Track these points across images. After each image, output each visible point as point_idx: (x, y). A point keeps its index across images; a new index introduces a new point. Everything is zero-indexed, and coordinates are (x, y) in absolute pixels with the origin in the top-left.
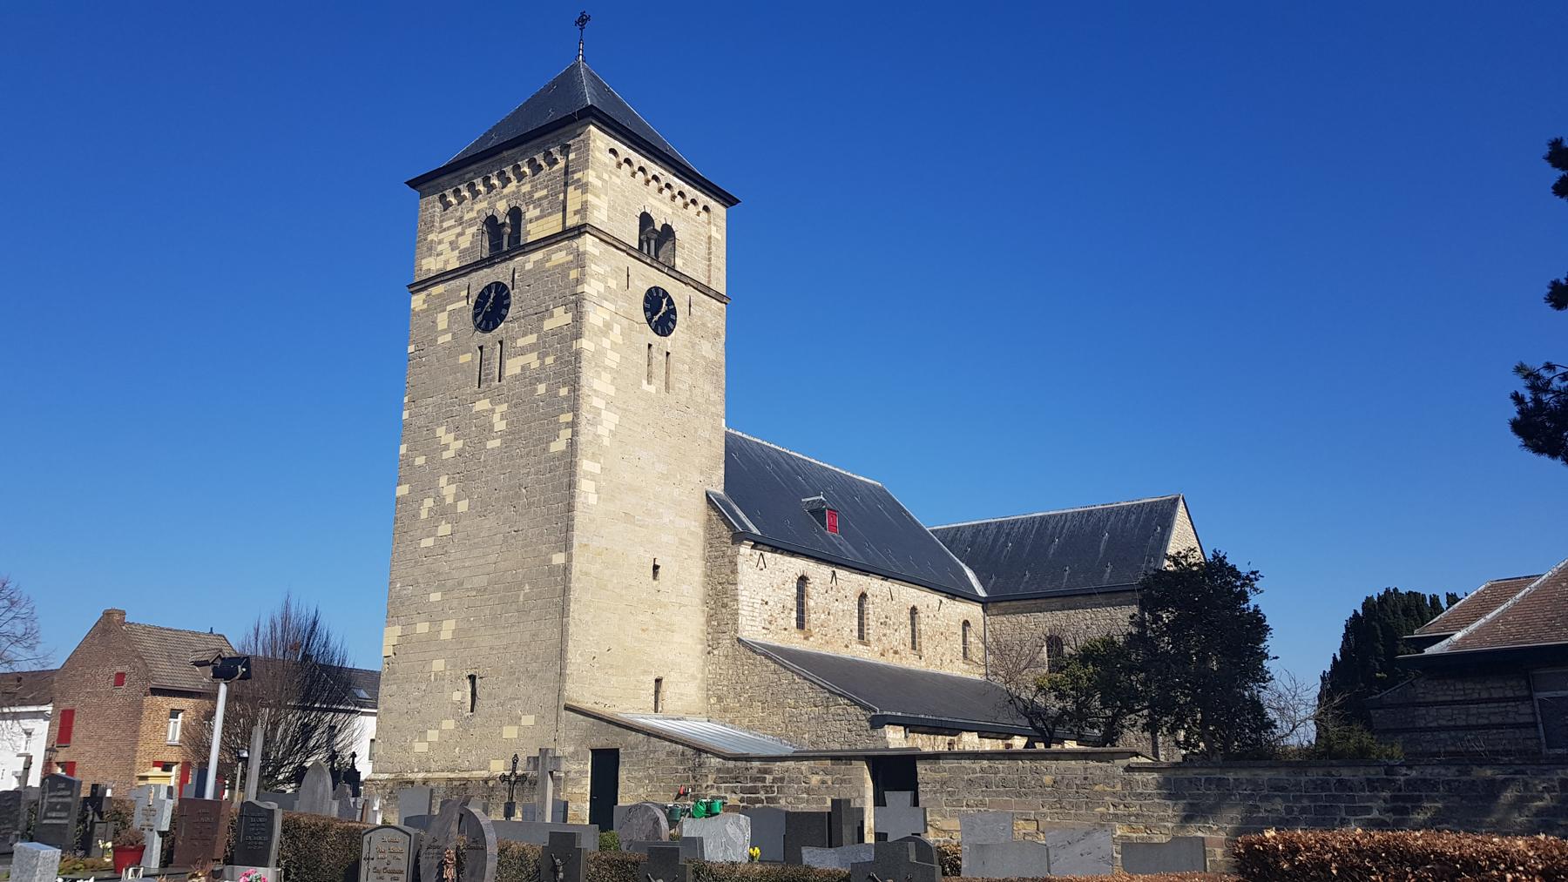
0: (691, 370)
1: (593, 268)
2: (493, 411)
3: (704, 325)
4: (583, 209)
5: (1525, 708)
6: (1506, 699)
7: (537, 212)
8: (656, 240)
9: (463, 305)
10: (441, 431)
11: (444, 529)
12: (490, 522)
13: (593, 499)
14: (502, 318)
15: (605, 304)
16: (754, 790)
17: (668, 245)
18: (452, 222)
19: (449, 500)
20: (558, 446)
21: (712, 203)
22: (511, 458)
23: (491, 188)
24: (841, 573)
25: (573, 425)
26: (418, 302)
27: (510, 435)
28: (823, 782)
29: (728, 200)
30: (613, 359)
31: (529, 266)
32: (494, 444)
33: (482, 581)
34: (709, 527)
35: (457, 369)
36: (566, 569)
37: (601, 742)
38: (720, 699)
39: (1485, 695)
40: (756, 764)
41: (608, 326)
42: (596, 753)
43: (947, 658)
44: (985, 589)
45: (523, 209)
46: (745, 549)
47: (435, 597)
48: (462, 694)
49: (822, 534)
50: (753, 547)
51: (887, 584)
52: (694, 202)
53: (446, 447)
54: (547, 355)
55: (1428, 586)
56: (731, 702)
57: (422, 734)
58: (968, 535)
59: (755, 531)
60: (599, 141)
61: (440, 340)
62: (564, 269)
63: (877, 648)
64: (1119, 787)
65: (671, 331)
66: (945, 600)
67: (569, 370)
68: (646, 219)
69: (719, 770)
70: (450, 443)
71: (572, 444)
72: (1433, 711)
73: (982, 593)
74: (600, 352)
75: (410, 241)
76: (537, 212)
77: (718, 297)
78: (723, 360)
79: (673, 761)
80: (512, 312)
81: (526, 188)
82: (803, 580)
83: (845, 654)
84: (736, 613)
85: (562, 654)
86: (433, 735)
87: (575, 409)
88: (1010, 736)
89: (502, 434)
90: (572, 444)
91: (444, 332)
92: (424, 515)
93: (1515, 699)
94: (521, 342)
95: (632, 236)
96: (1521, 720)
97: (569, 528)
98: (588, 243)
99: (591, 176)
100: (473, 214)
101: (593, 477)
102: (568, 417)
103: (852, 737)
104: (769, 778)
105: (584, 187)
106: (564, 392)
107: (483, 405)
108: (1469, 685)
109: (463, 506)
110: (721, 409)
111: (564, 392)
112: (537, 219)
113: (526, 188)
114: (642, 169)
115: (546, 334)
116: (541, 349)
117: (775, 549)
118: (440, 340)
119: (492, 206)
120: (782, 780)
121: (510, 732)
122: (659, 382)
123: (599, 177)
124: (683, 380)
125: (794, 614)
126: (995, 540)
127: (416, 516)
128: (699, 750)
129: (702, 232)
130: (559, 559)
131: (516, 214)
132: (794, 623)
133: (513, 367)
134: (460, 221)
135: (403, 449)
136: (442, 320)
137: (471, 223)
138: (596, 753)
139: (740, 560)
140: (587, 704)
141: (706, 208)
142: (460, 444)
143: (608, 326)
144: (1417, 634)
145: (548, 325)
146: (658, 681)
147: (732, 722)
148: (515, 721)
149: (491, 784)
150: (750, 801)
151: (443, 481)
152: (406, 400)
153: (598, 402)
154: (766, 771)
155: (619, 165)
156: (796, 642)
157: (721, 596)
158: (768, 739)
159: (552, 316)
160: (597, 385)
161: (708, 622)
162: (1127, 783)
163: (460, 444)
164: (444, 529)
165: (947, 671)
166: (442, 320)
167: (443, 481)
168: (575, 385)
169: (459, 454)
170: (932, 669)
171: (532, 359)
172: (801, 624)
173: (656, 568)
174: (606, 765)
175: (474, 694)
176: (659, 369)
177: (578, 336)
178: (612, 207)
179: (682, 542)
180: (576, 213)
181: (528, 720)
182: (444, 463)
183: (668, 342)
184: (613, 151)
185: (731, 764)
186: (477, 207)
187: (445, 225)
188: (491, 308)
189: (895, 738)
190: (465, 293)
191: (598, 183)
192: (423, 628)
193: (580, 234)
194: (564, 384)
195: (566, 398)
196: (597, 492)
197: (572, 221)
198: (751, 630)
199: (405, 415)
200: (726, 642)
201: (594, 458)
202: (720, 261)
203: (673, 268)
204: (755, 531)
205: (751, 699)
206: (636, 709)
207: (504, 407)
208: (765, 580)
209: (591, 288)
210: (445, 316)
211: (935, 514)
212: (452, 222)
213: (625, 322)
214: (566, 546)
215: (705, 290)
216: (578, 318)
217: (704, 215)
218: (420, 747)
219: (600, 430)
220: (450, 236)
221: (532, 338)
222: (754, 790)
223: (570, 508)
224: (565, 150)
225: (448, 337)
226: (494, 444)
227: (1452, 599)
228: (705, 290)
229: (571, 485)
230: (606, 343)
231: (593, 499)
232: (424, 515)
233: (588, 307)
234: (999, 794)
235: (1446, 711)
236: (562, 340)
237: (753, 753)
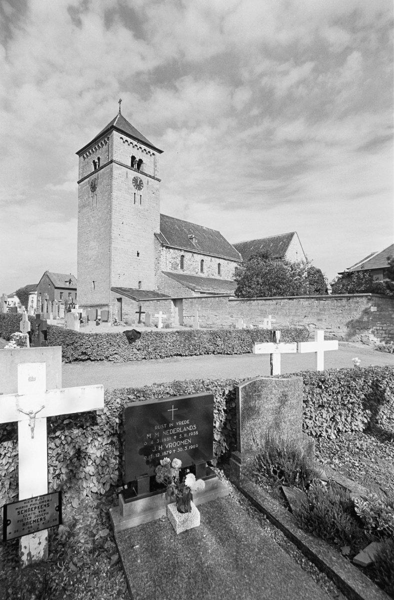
52: (149, 152)
68: (133, 158)
114: (131, 143)
155: (124, 142)
156: (181, 272)
172: (182, 267)
173: (138, 254)
184: (121, 138)
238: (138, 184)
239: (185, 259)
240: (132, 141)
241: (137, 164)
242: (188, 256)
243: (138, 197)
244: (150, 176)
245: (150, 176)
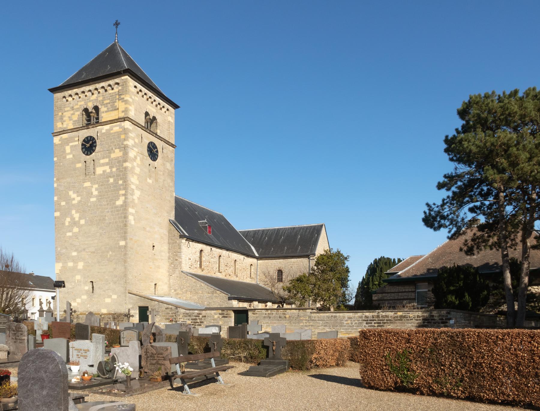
0: (163, 174)
1: (131, 135)
2: (92, 187)
3: (167, 156)
5: (413, 294)
6: (409, 292)
7: (106, 109)
8: (151, 122)
9: (78, 144)
10: (71, 193)
11: (76, 230)
14: (94, 151)
15: (135, 149)
16: (196, 319)
18: (69, 109)
19: (77, 219)
20: (119, 202)
21: (170, 108)
22: (101, 205)
24: (214, 249)
26: (56, 140)
27: (100, 197)
28: (219, 317)
29: (175, 106)
31: (104, 131)
32: (93, 200)
33: (93, 249)
34: (170, 231)
35: (75, 169)
37: (142, 304)
38: (175, 290)
39: (404, 290)
40: (196, 311)
42: (140, 308)
43: (245, 277)
44: (258, 253)
45: (100, 107)
47: (74, 254)
48: (88, 287)
49: (206, 234)
50: (186, 240)
51: (228, 252)
53: (74, 199)
54: (113, 167)
55: (392, 255)
56: (179, 291)
58: (252, 234)
59: (187, 234)
60: (131, 82)
61: (68, 157)
62: (119, 134)
63: (224, 274)
64: (307, 318)
65: (156, 159)
66: (245, 257)
67: (123, 174)
68: (147, 114)
69: (184, 314)
70: (76, 199)
72: (389, 295)
73: (257, 255)
74: (133, 168)
75: (50, 114)
76: (106, 109)
77: (173, 146)
78: (174, 170)
79: (168, 311)
80: (98, 149)
82: (201, 251)
83: (214, 276)
84: (180, 263)
87: (126, 189)
88: (267, 302)
89: (96, 196)
90: (125, 202)
91: (69, 154)
93: (412, 292)
94: (102, 161)
95: (142, 120)
96: (412, 297)
97: (125, 233)
100: (78, 107)
101: (133, 215)
102: (123, 192)
103: (221, 303)
104: (201, 316)
106: (121, 182)
107: (87, 184)
108: (400, 287)
109: (82, 222)
110: (173, 189)
111: (121, 182)
112: (106, 112)
113: (101, 98)
114: (145, 94)
115: (112, 159)
116: (111, 164)
117: (193, 241)
118: (68, 157)
119: (86, 104)
120: (205, 316)
121: (108, 300)
123: (131, 98)
125: (199, 263)
126: (262, 236)
127: (64, 224)
128: (177, 307)
129: (166, 118)
130: (122, 243)
131: (96, 108)
132: (199, 266)
133: (99, 171)
134: (72, 108)
135: (56, 198)
137: (77, 110)
138: (140, 308)
139: (182, 244)
140: (135, 292)
141: (168, 110)
142: (79, 198)
144: (388, 272)
145: (113, 156)
146: (155, 284)
147: (180, 298)
148: (110, 297)
149: (103, 316)
150: (194, 322)
152: (55, 179)
153: (133, 187)
154: (200, 314)
158: (193, 303)
159: (114, 152)
160: (134, 180)
161: (170, 265)
162: (310, 317)
163: (79, 198)
165: (245, 281)
166: (68, 149)
167: (73, 212)
168: (125, 181)
169: (80, 202)
170: (240, 280)
173: (154, 246)
174: (144, 312)
175: (93, 287)
178: (136, 110)
179: (162, 238)
180: (123, 112)
181: (115, 297)
182: (73, 205)
183: (156, 163)
184: (135, 87)
185: (188, 312)
186: (79, 104)
187: (66, 109)
188: (89, 146)
189: (235, 304)
190: (77, 139)
191: (130, 100)
192: (70, 264)
193: (125, 121)
194: (121, 179)
195: (122, 185)
196: (134, 220)
199: (55, 185)
201: (133, 207)
203: (156, 134)
204: (187, 234)
205: (186, 291)
206: (149, 293)
207: (96, 186)
208: (191, 250)
210: (71, 147)
211: (241, 225)
212: (69, 109)
213: (141, 156)
215: (168, 143)
217: (167, 112)
219: (135, 197)
221: (107, 160)
222: (196, 319)
225: (71, 156)
226: (93, 200)
227: (399, 261)
228: (168, 143)
229: (126, 217)
230: (135, 164)
231: (133, 222)
232: (67, 224)
233: (129, 150)
234: (273, 320)
235: (393, 295)
236: (119, 162)
237: (195, 308)
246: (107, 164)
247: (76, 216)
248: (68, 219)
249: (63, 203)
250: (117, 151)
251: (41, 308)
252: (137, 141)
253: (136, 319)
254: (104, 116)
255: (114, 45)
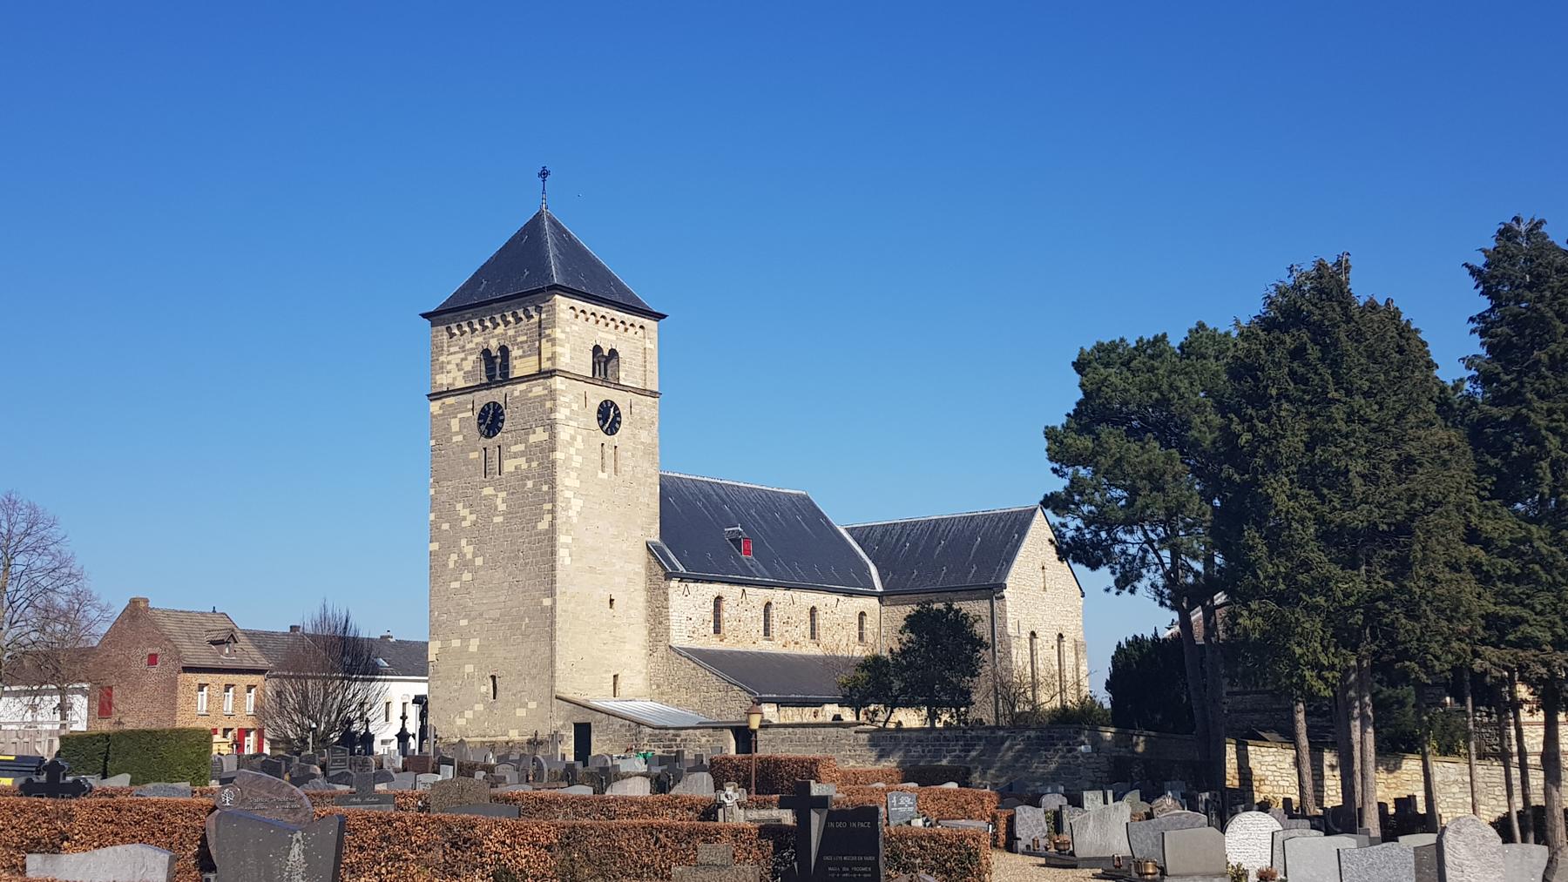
1: (561, 399)
4: (552, 358)
7: (520, 352)
9: (471, 416)
10: (459, 506)
11: (467, 576)
12: (499, 574)
13: (568, 561)
17: (613, 362)
19: (469, 556)
20: (543, 525)
23: (485, 328)
25: (552, 512)
30: (577, 461)
31: (516, 393)
35: (467, 462)
36: (553, 608)
41: (573, 438)
46: (674, 583)
47: (464, 623)
53: (464, 519)
57: (461, 714)
61: (455, 439)
67: (548, 473)
71: (552, 524)
74: (569, 458)
76: (520, 352)
80: (506, 425)
81: (511, 332)
85: (552, 663)
86: (469, 714)
87: (553, 501)
90: (552, 524)
91: (457, 433)
92: (451, 565)
94: (514, 449)
97: (553, 582)
98: (558, 383)
99: (558, 333)
102: (548, 506)
105: (553, 341)
106: (545, 488)
107: (488, 491)
109: (479, 561)
111: (545, 488)
113: (511, 332)
116: (528, 454)
118: (455, 439)
121: (521, 712)
122: (610, 469)
124: (627, 464)
127: (446, 565)
130: (547, 602)
131: (504, 350)
133: (509, 466)
136: (455, 425)
140: (569, 696)
142: (473, 517)
143: (573, 438)
145: (532, 439)
148: (524, 705)
151: (463, 542)
153: (568, 494)
157: (658, 616)
160: (567, 482)
163: (473, 517)
164: (467, 576)
166: (455, 425)
167: (463, 542)
169: (474, 524)
171: (522, 462)
174: (583, 733)
176: (610, 460)
177: (553, 450)
181: (533, 705)
188: (491, 420)
192: (456, 643)
197: (546, 365)
198: (679, 637)
200: (662, 648)
201: (567, 533)
202: (653, 366)
209: (561, 414)
214: (552, 594)
216: (553, 436)
218: (460, 722)
220: (458, 361)
221: (521, 447)
223: (553, 569)
224: (539, 310)
225: (460, 438)
229: (553, 553)
230: (572, 451)
232: (451, 565)
233: (559, 428)
238: (608, 418)
239: (724, 605)
240: (594, 308)
241: (605, 361)
242: (731, 593)
243: (609, 452)
244: (636, 391)
245: (636, 391)
246: (522, 454)
247: (469, 550)
248: (454, 557)
249: (445, 526)
250: (539, 430)
251: (403, 729)
252: (575, 407)
253: (568, 749)
254: (521, 366)
255: (533, 228)
